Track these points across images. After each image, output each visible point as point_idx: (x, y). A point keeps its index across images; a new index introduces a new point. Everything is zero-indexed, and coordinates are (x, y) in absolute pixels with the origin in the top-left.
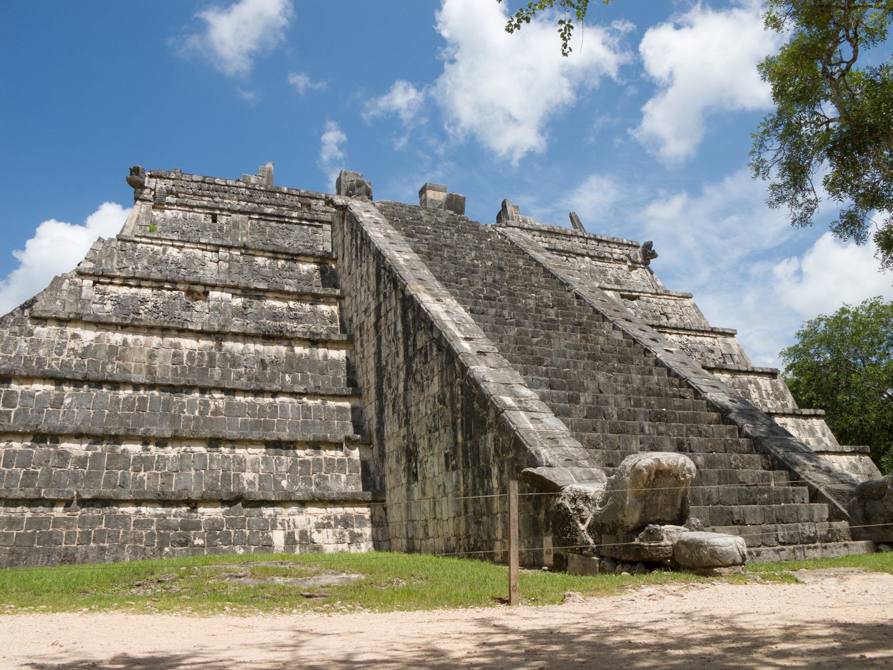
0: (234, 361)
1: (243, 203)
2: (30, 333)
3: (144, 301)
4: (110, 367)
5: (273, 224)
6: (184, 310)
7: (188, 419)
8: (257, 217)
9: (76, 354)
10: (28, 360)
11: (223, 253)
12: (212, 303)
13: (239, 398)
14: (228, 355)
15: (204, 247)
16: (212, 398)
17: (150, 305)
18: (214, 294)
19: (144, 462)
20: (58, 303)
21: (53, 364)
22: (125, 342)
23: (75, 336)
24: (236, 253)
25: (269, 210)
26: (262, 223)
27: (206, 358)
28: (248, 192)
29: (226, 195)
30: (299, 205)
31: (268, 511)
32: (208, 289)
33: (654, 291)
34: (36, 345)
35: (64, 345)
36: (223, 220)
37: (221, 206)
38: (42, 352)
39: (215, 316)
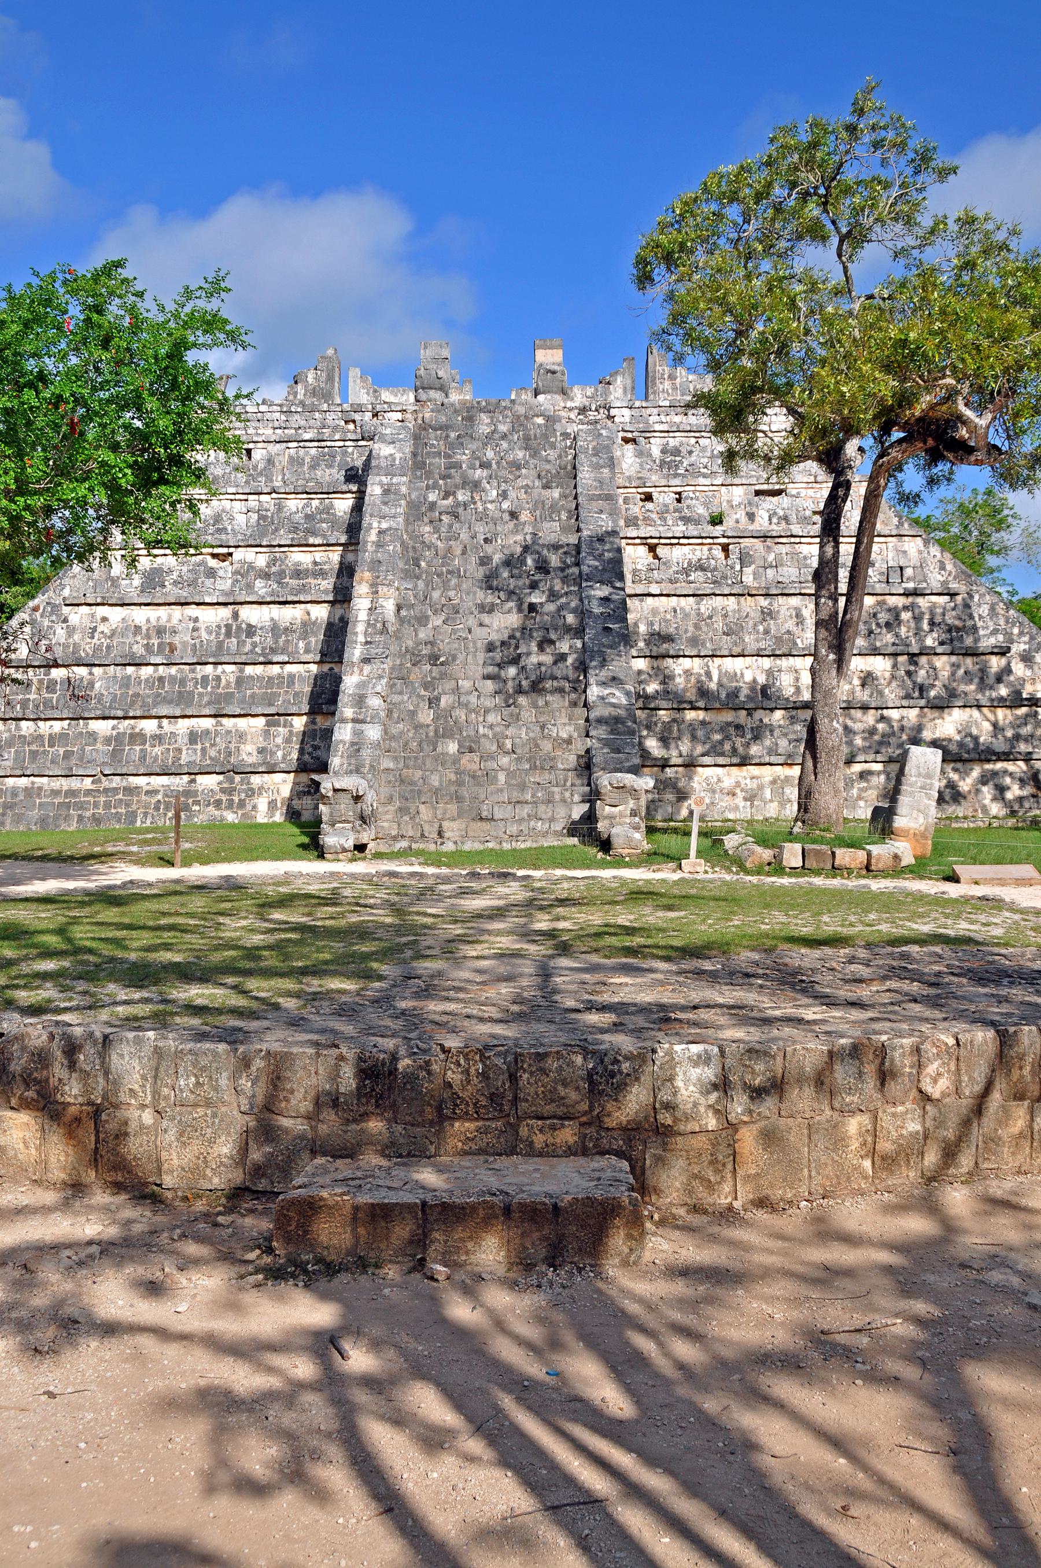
0: (251, 631)
1: (278, 431)
2: (65, 621)
3: (170, 571)
4: (135, 647)
5: (313, 451)
6: (208, 577)
7: (201, 695)
8: (295, 444)
9: (105, 637)
10: (66, 646)
11: (253, 501)
12: (235, 566)
13: (249, 670)
14: (244, 626)
15: (232, 497)
16: (224, 672)
17: (175, 576)
18: (238, 554)
19: (158, 738)
20: (91, 583)
21: (86, 649)
22: (148, 621)
23: (104, 619)
24: (264, 498)
25: (307, 436)
26: (302, 451)
27: (223, 630)
28: (283, 418)
29: (260, 425)
30: (343, 423)
31: (256, 780)
32: (231, 550)
33: (812, 479)
34: (71, 631)
35: (94, 629)
36: (257, 455)
37: (255, 439)
38: (77, 637)
39: (237, 581)
